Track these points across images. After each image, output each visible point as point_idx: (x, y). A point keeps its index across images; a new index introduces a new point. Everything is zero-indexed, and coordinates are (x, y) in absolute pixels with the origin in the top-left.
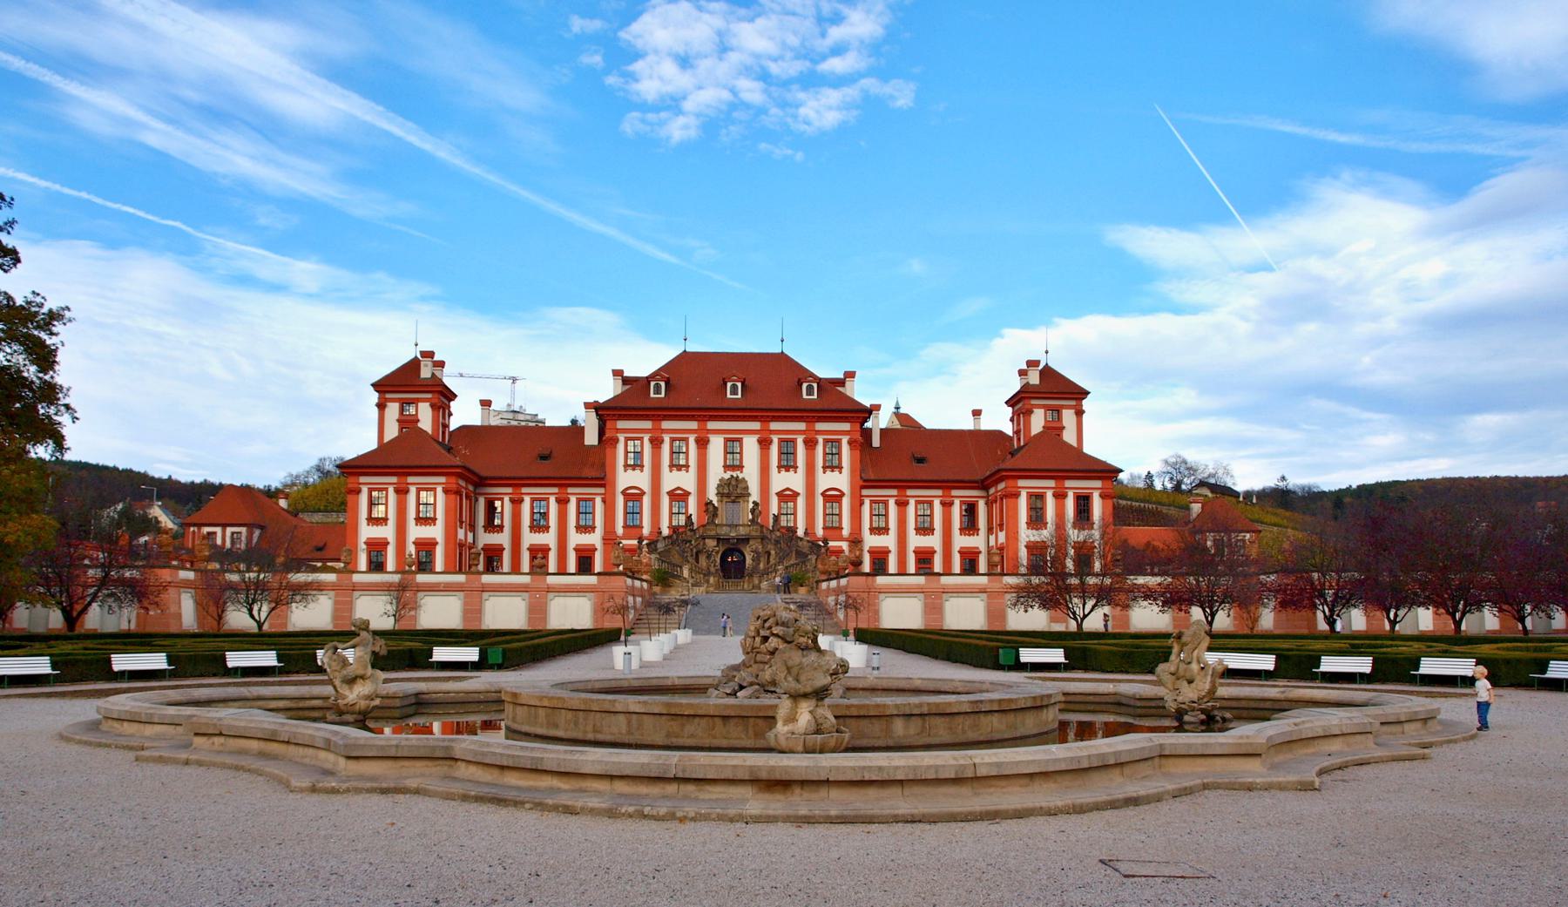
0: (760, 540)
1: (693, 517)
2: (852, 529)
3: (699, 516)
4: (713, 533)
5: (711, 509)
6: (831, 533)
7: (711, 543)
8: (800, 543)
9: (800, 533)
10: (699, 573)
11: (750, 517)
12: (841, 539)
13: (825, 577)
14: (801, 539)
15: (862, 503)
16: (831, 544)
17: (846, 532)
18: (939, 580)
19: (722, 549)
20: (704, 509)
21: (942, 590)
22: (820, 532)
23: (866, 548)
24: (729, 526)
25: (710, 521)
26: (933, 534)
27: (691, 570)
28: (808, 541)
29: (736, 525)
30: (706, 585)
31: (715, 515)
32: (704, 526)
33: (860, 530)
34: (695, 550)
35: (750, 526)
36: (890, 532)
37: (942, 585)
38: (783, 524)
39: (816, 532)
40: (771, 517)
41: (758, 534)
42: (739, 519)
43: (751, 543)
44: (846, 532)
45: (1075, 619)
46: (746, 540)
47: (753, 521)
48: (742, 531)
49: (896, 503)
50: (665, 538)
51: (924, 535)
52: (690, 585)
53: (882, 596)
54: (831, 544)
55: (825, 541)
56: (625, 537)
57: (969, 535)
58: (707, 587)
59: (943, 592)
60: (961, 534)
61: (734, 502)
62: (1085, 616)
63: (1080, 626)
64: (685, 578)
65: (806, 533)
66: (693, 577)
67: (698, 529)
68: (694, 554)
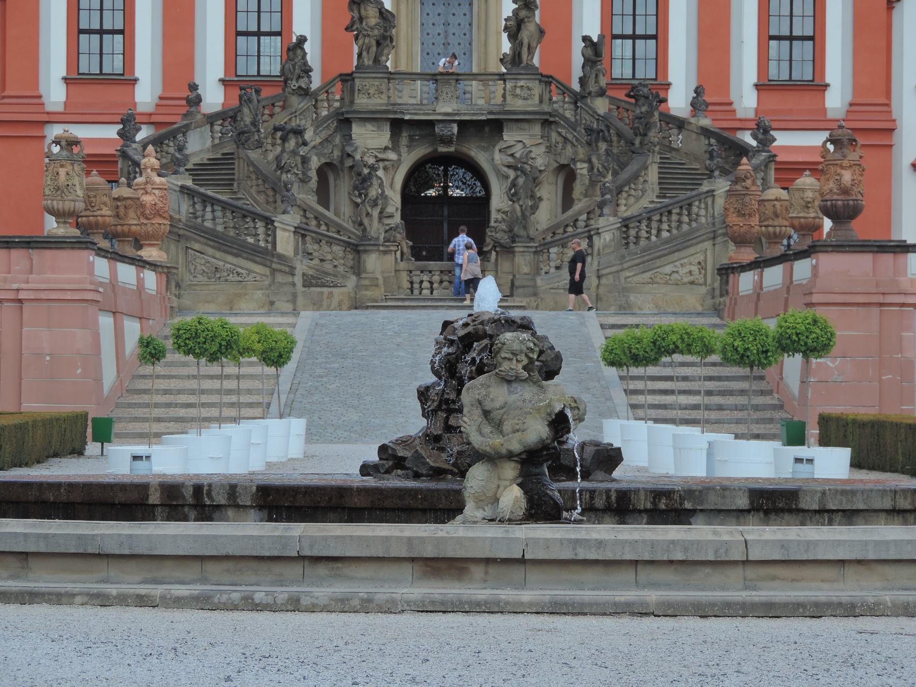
0: (537, 129)
2: (857, 87)
6: (775, 101)
8: (678, 140)
10: (331, 241)
11: (506, 47)
13: (748, 255)
14: (680, 124)
16: (782, 139)
19: (409, 159)
24: (434, 77)
25: (368, 61)
27: (301, 232)
28: (706, 132)
29: (457, 77)
30: (352, 281)
31: (385, 41)
32: (347, 79)
33: (888, 93)
34: (315, 163)
35: (502, 77)
38: (621, 70)
40: (578, 46)
42: (468, 54)
43: (509, 136)
47: (515, 60)
50: (211, 119)
52: (298, 280)
54: (782, 139)
55: (763, 131)
56: (69, 116)
58: (358, 287)
64: (281, 257)
65: (697, 104)
66: (309, 255)
67: (326, 87)
68: (313, 174)
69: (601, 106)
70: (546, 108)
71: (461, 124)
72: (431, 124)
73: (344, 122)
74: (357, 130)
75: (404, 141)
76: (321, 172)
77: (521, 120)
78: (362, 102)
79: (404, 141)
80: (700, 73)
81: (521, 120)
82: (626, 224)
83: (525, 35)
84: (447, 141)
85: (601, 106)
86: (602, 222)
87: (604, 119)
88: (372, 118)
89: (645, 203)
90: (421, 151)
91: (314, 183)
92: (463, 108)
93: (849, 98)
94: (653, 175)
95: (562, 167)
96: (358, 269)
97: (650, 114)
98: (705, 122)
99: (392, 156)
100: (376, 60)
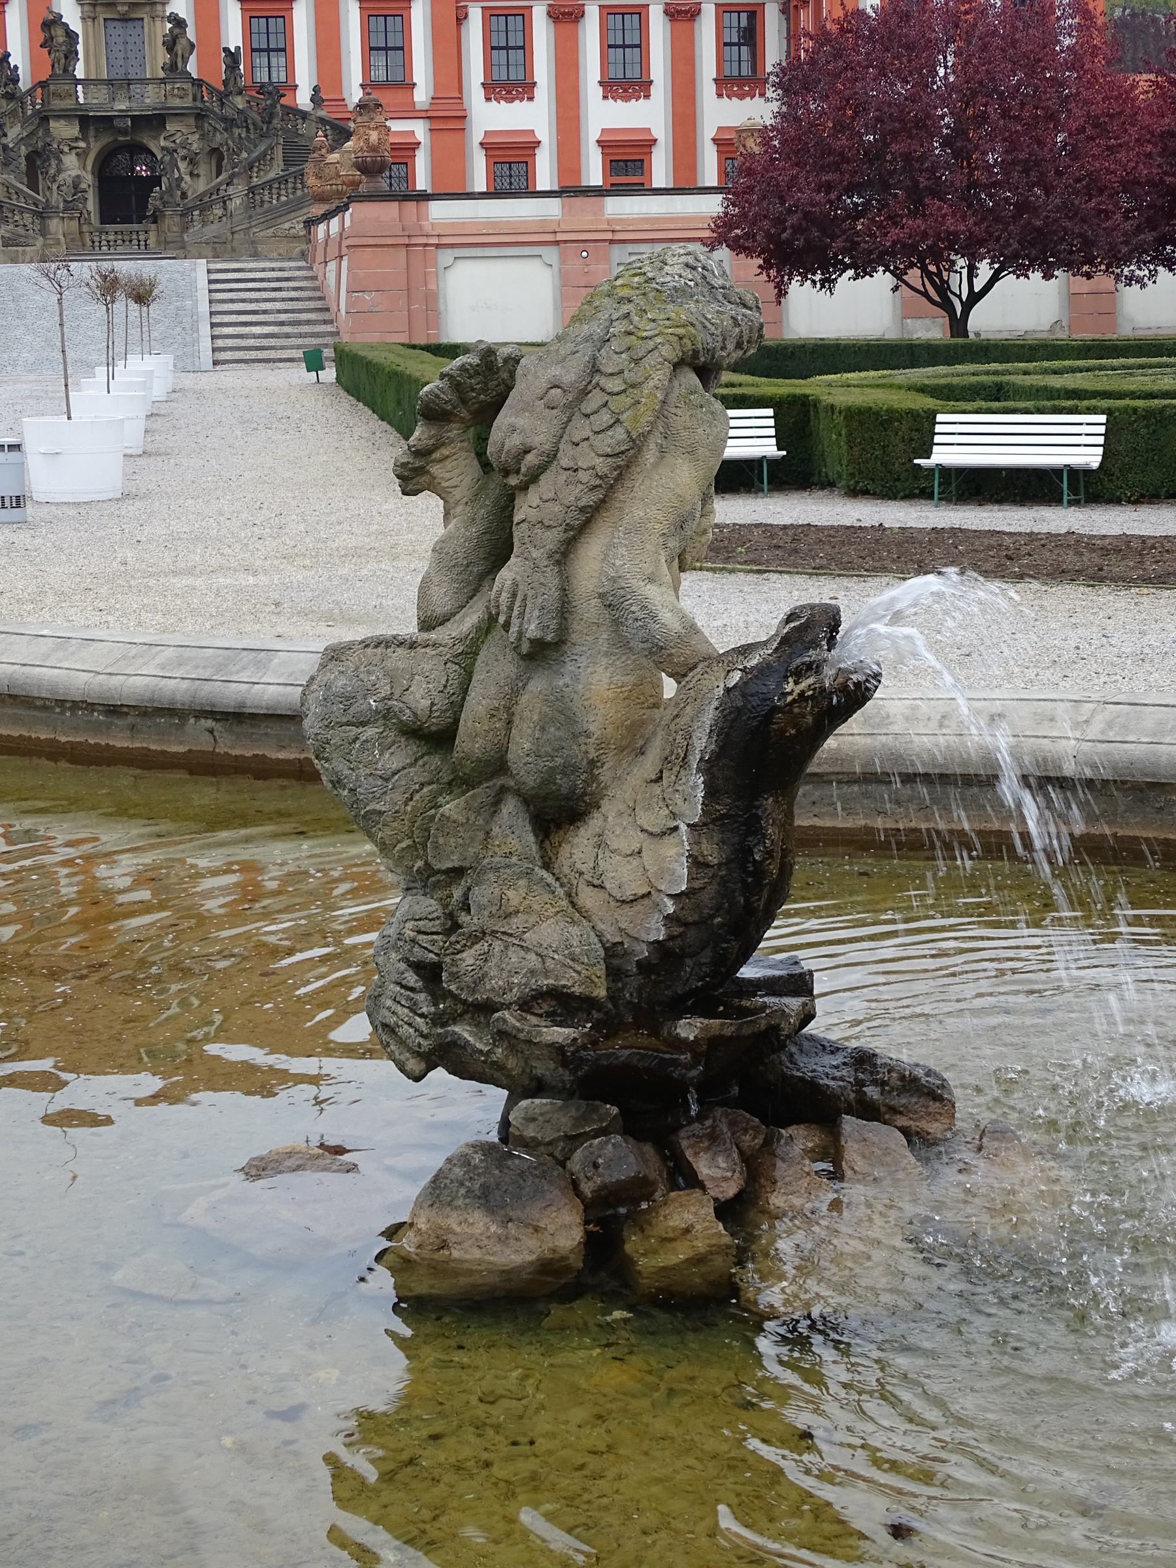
0: (191, 121)
1: (20, 72)
2: (436, 86)
3: (34, 61)
4: (68, 104)
5: (60, 38)
7: (64, 130)
8: (303, 128)
9: (303, 99)
10: (22, 210)
11: (163, 57)
12: (411, 113)
14: (304, 115)
15: (461, 18)
17: (421, 96)
18: (602, 208)
19: (96, 146)
20: (41, 37)
21: (609, 236)
22: (354, 94)
23: (477, 136)
24: (109, 82)
25: (59, 71)
26: (647, 96)
28: (322, 121)
29: (129, 82)
30: (40, 241)
31: (71, 55)
32: (43, 85)
33: (460, 90)
34: (24, 151)
35: (163, 81)
36: (537, 92)
37: (609, 222)
38: (262, 76)
39: (345, 96)
41: (188, 102)
42: (142, 65)
43: (170, 127)
44: (421, 96)
45: (947, 305)
46: (156, 121)
48: (150, 98)
49: (549, 14)
51: (626, 99)
53: (445, 257)
57: (741, 97)
58: (44, 245)
59: (612, 242)
60: (720, 95)
61: (125, 19)
62: (975, 298)
63: (959, 325)
65: (316, 99)
67: (31, 92)
68: (23, 160)
69: (240, 102)
70: (199, 105)
71: (133, 118)
72: (111, 118)
73: (44, 119)
74: (52, 123)
75: (92, 132)
76: (29, 158)
77: (179, 115)
78: (57, 104)
79: (92, 132)
80: (319, 77)
81: (179, 115)
82: (252, 190)
83: (179, 49)
84: (124, 132)
85: (240, 102)
86: (231, 190)
87: (240, 112)
88: (64, 115)
89: (272, 175)
90: (106, 140)
91: (23, 167)
92: (134, 105)
93: (431, 94)
94: (279, 153)
95: (214, 151)
96: (44, 232)
97: (273, 106)
98: (322, 113)
99: (82, 144)
100: (65, 70)
